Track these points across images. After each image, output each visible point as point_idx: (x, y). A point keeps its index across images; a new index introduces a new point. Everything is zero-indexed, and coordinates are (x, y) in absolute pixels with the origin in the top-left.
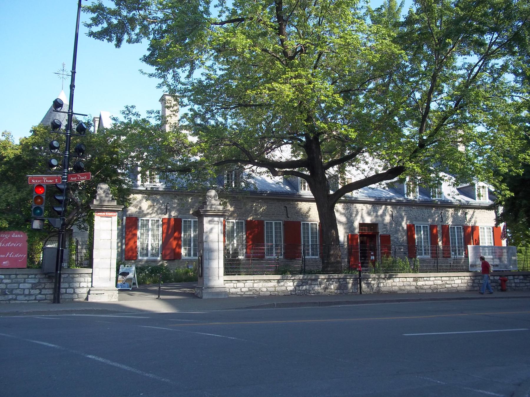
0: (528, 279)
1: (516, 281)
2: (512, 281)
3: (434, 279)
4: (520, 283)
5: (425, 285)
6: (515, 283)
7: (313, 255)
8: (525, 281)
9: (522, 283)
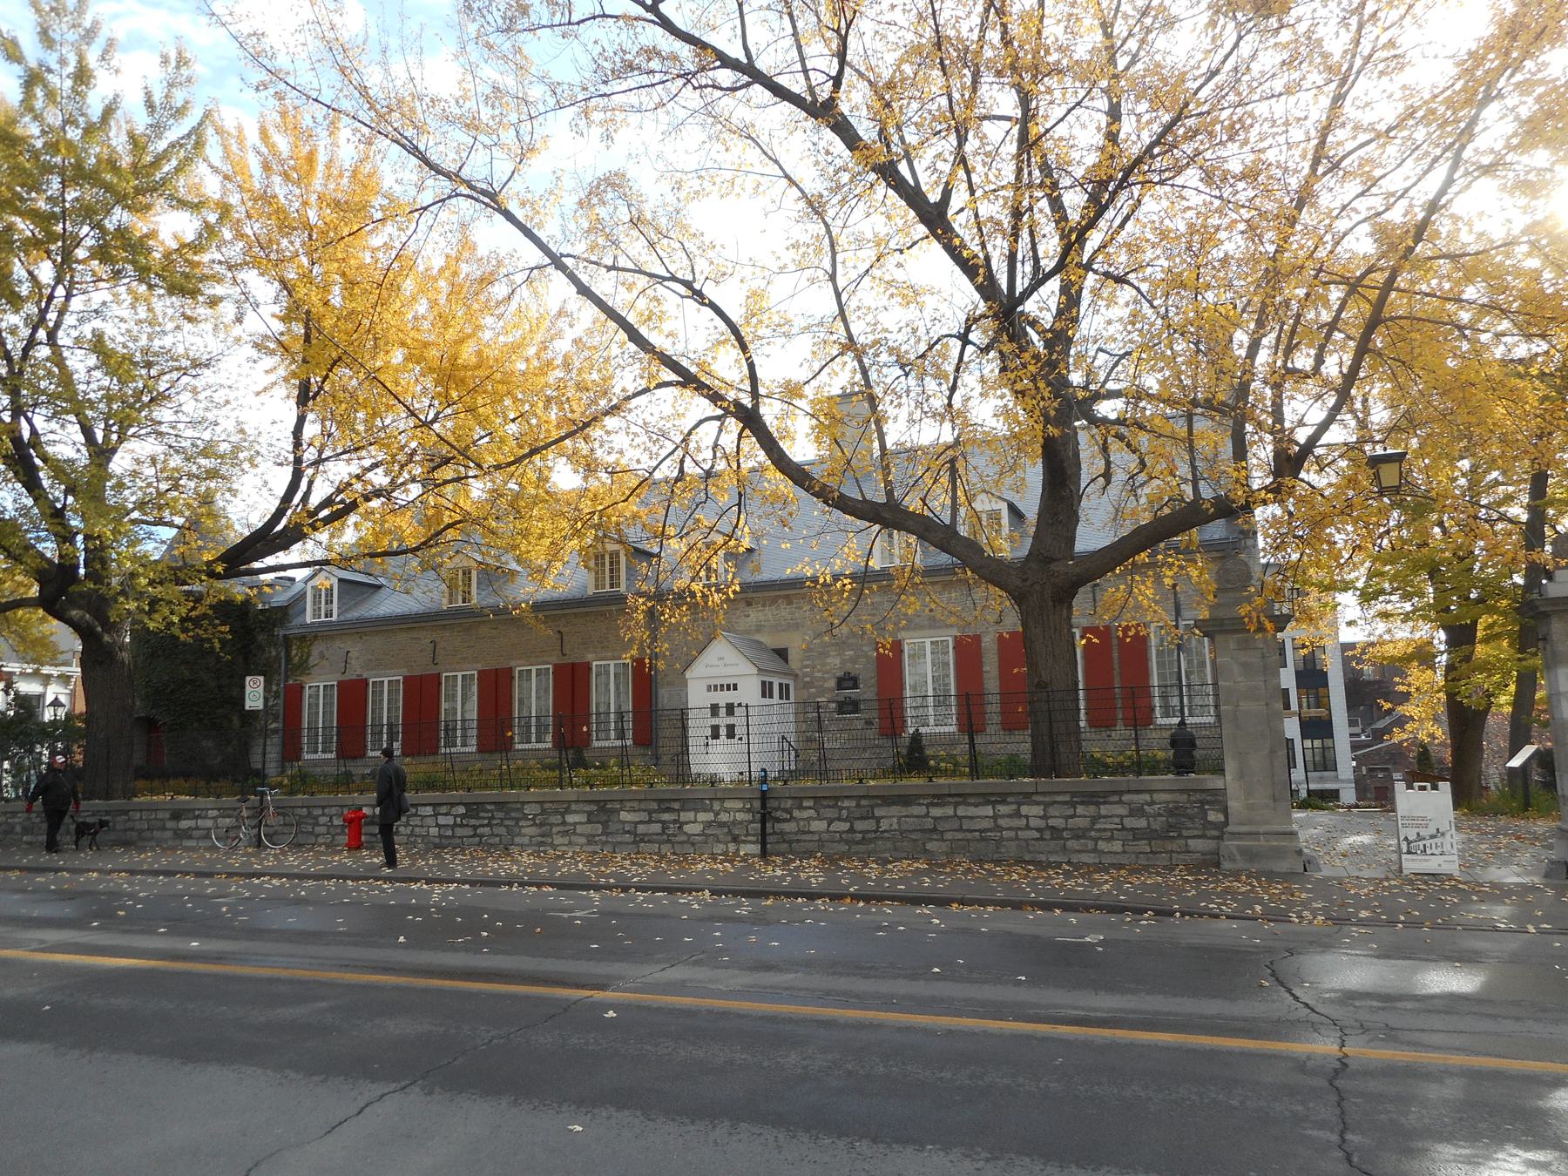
0: (482, 814)
1: (442, 820)
2: (430, 821)
3: (215, 813)
4: (455, 825)
5: (197, 828)
6: (437, 825)
7: (324, 751)
8: (473, 822)
9: (462, 826)
